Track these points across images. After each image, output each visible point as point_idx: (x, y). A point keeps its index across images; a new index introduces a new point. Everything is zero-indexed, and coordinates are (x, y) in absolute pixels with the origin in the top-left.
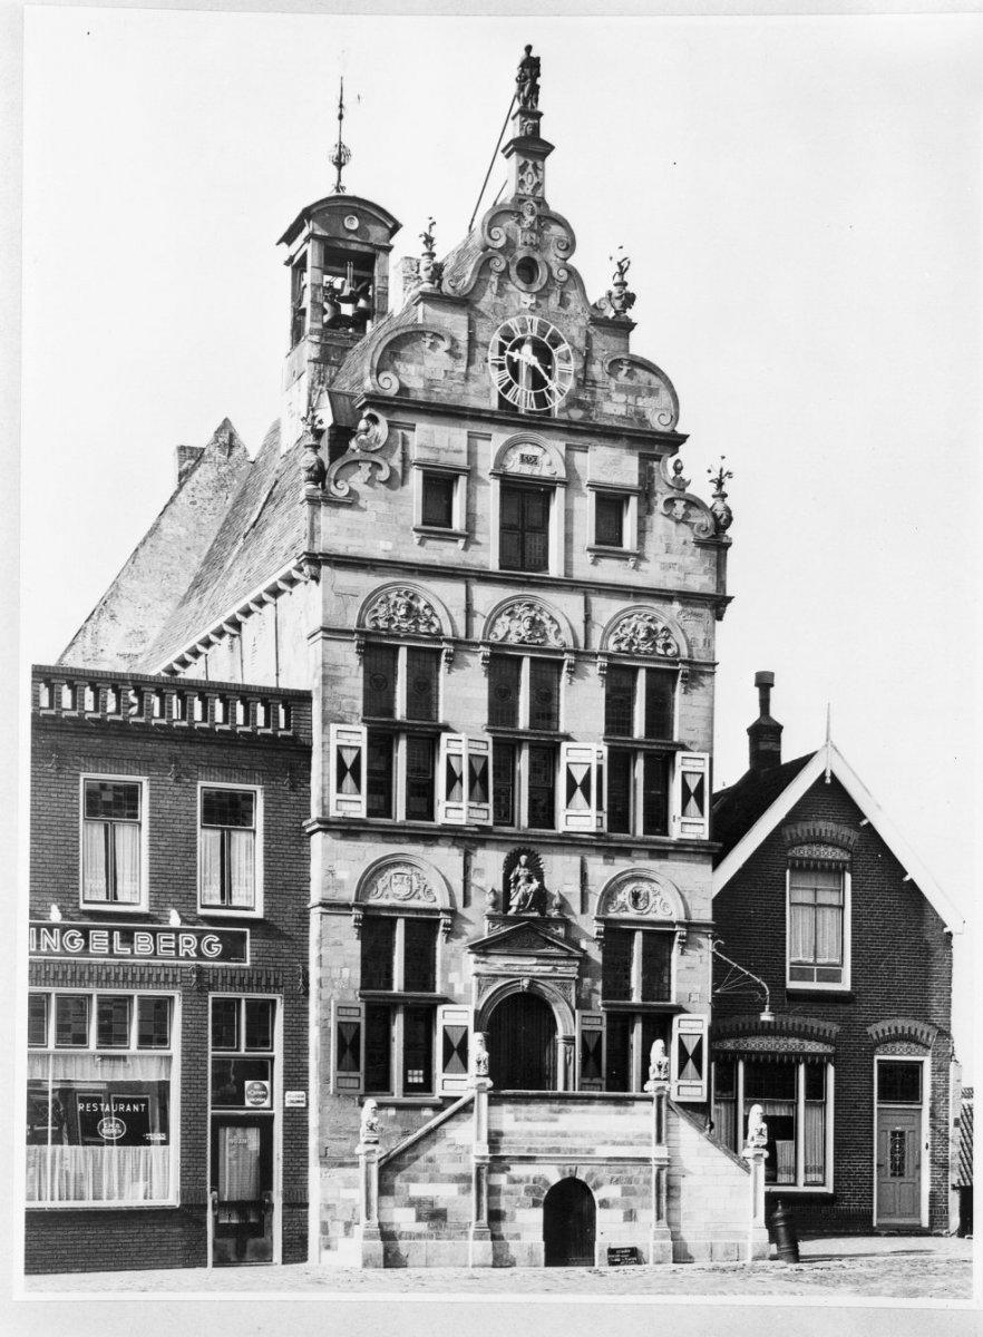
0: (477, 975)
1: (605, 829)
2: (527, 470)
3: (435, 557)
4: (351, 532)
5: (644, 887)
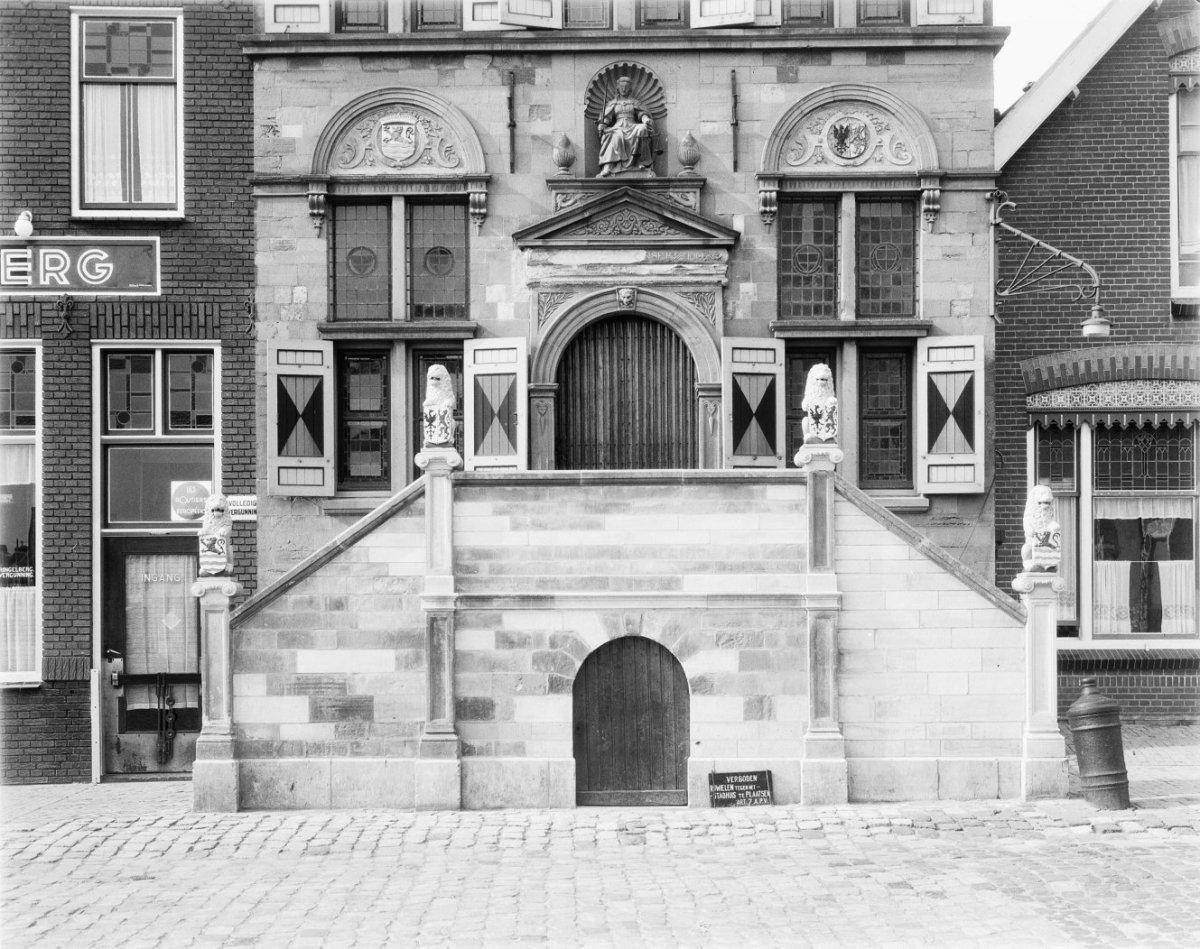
0: (533, 285)
5: (859, 118)
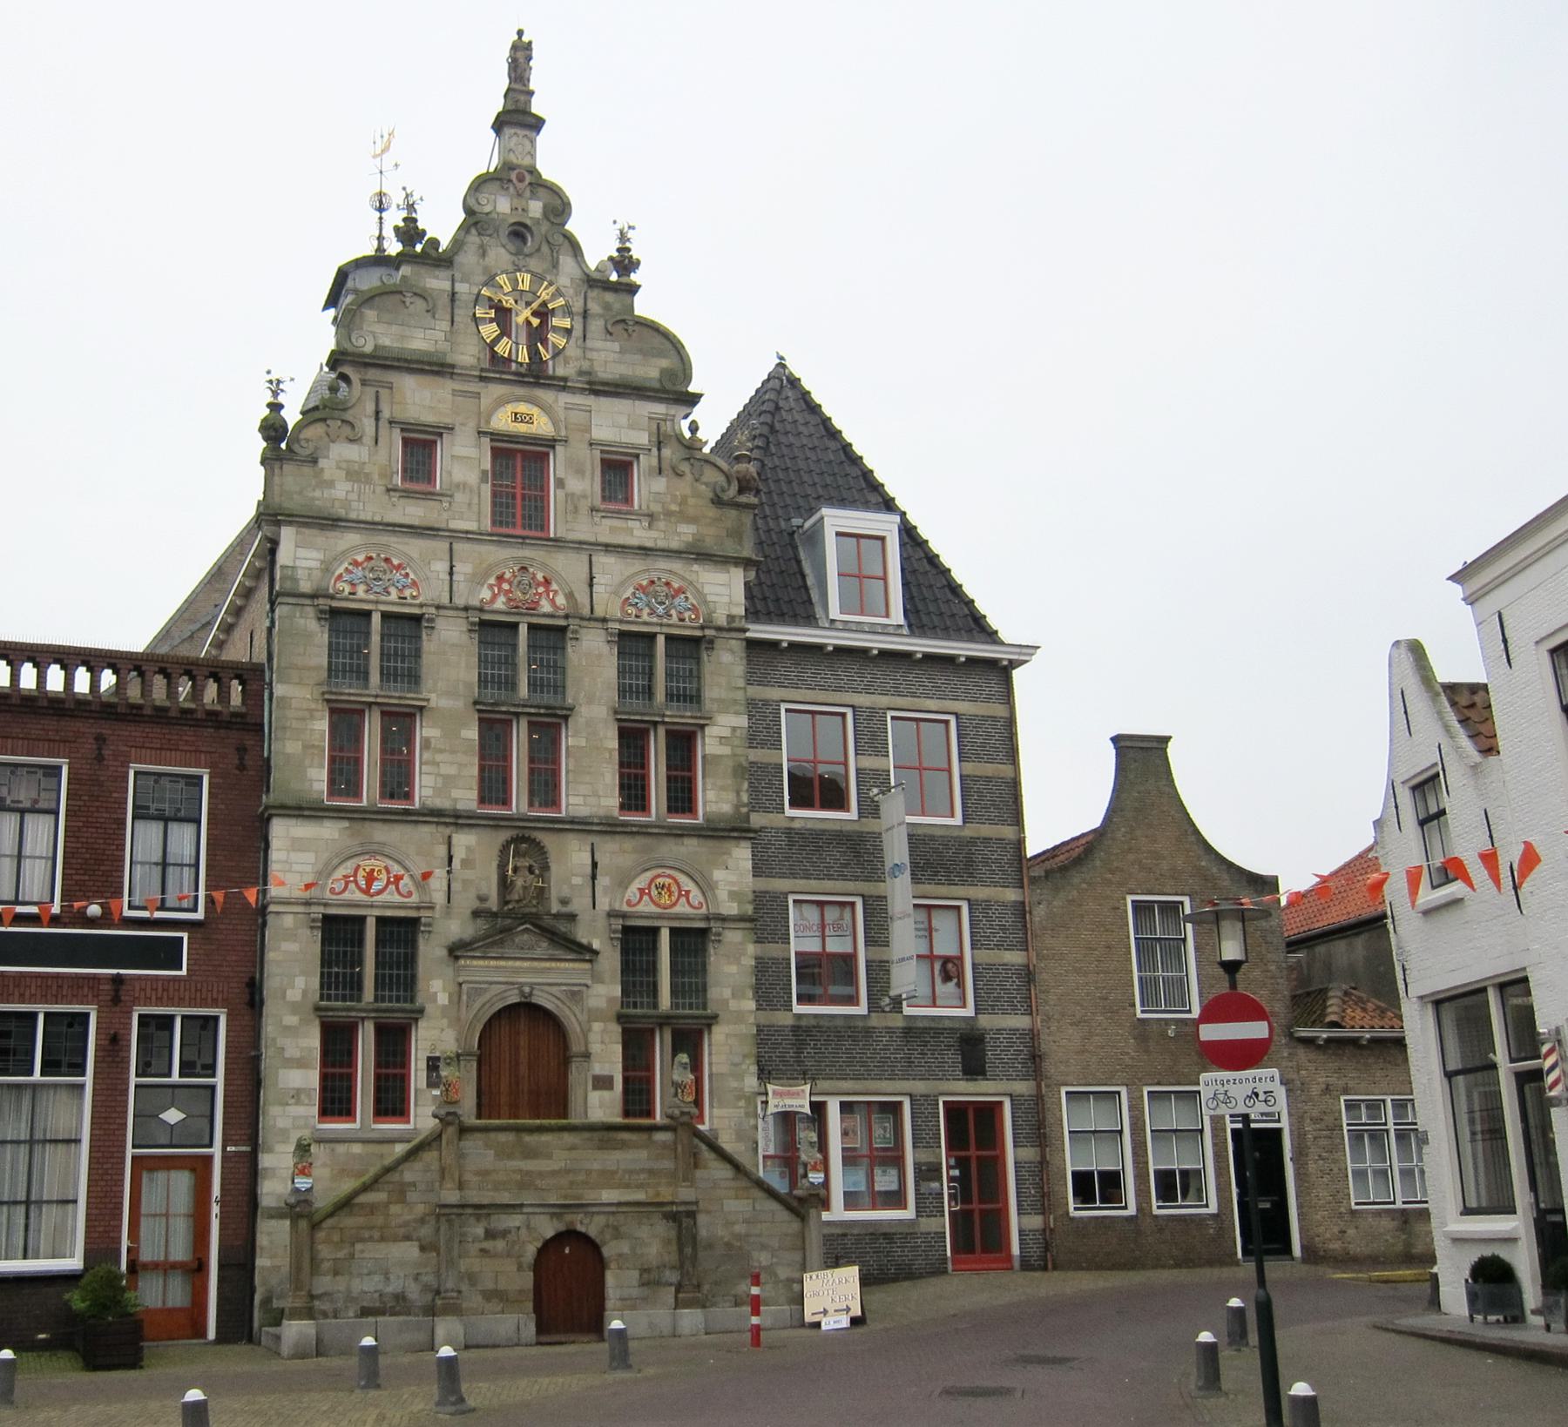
2: (522, 428)
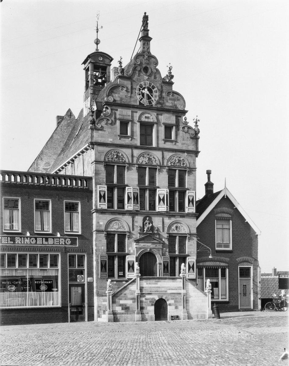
0: (136, 248)
1: (168, 210)
2: (147, 120)
3: (124, 143)
4: (102, 137)
5: (179, 225)
